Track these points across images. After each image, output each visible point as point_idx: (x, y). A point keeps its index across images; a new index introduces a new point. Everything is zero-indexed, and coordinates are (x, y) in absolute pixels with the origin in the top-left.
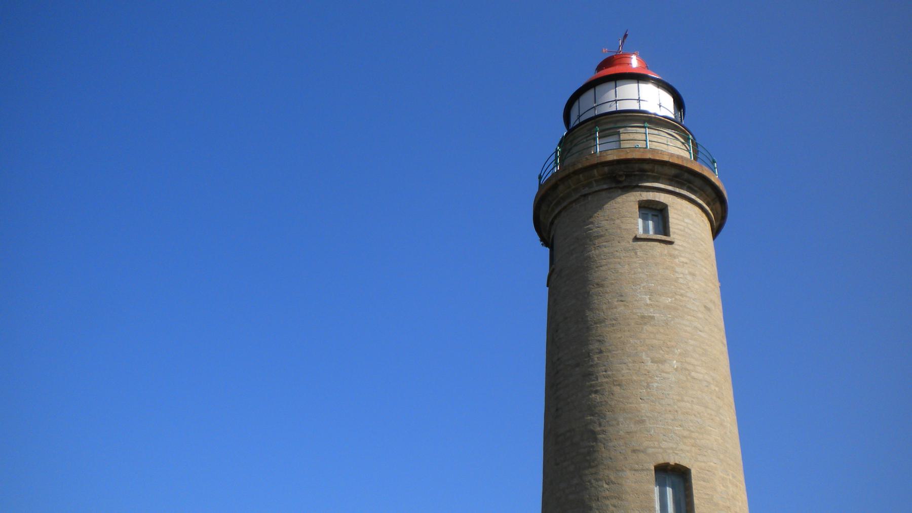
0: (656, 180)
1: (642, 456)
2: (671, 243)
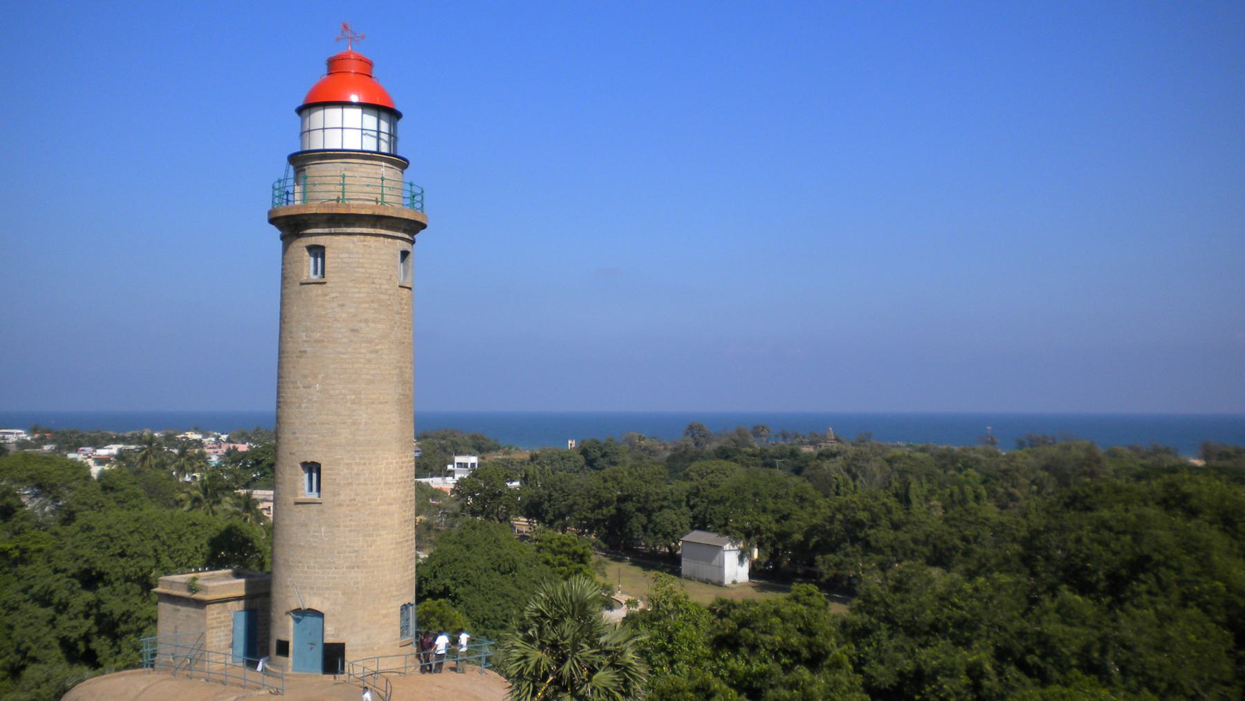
0: (317, 226)
1: (293, 456)
2: (325, 283)
